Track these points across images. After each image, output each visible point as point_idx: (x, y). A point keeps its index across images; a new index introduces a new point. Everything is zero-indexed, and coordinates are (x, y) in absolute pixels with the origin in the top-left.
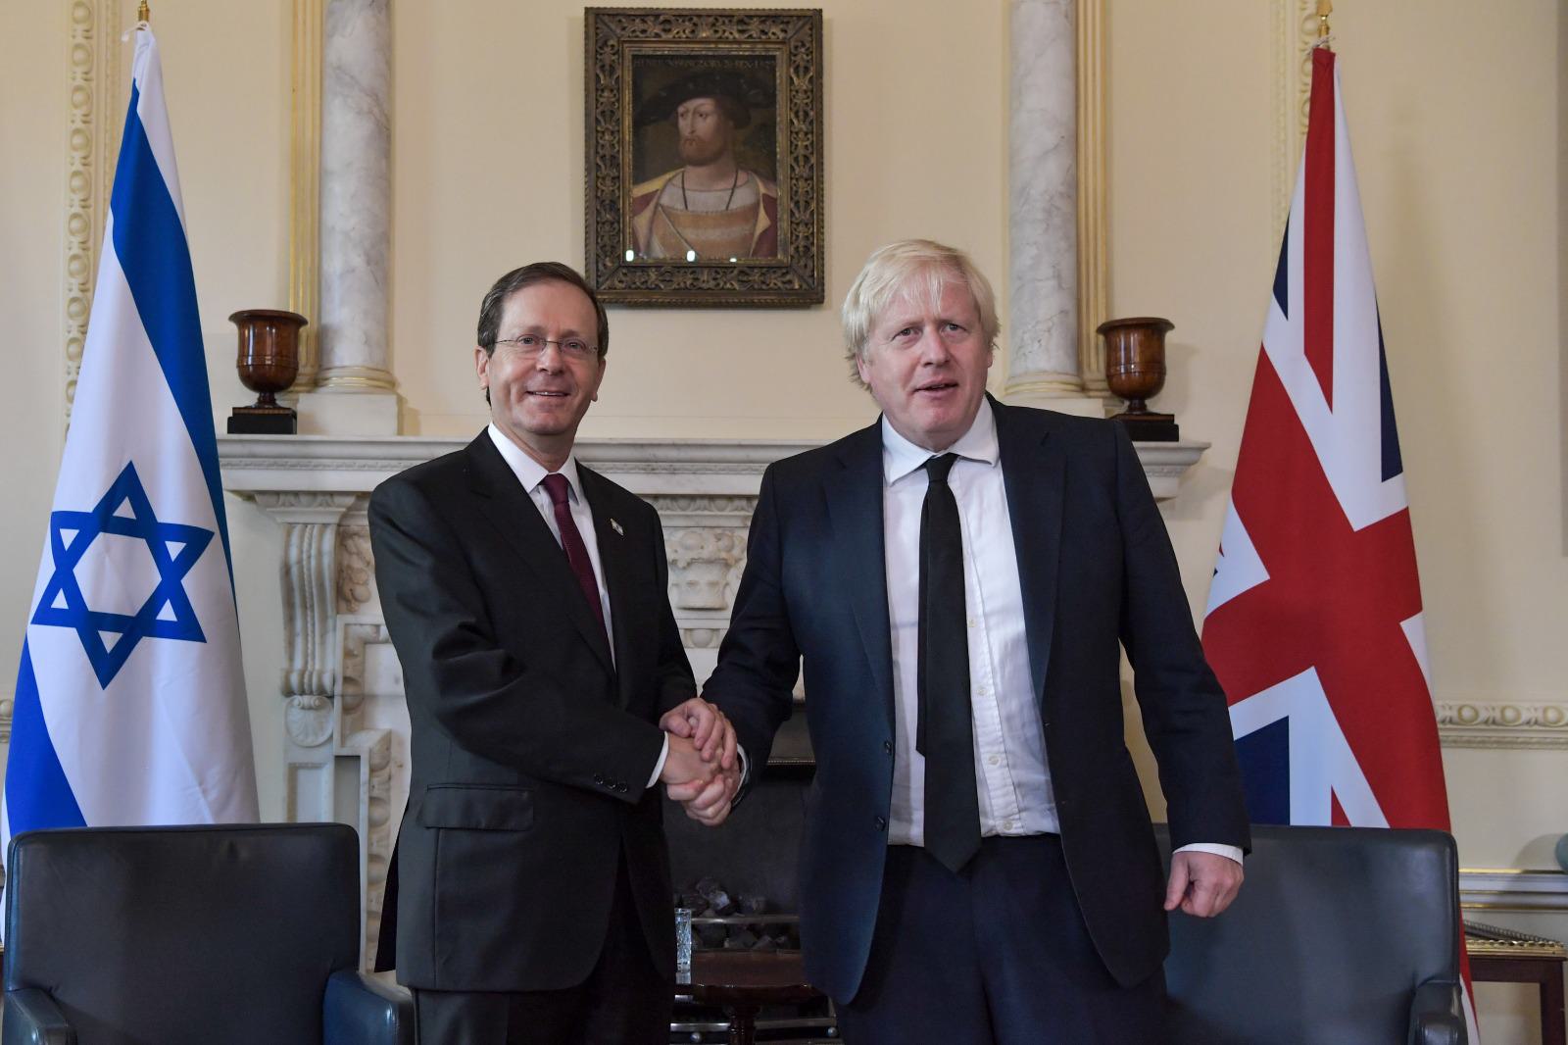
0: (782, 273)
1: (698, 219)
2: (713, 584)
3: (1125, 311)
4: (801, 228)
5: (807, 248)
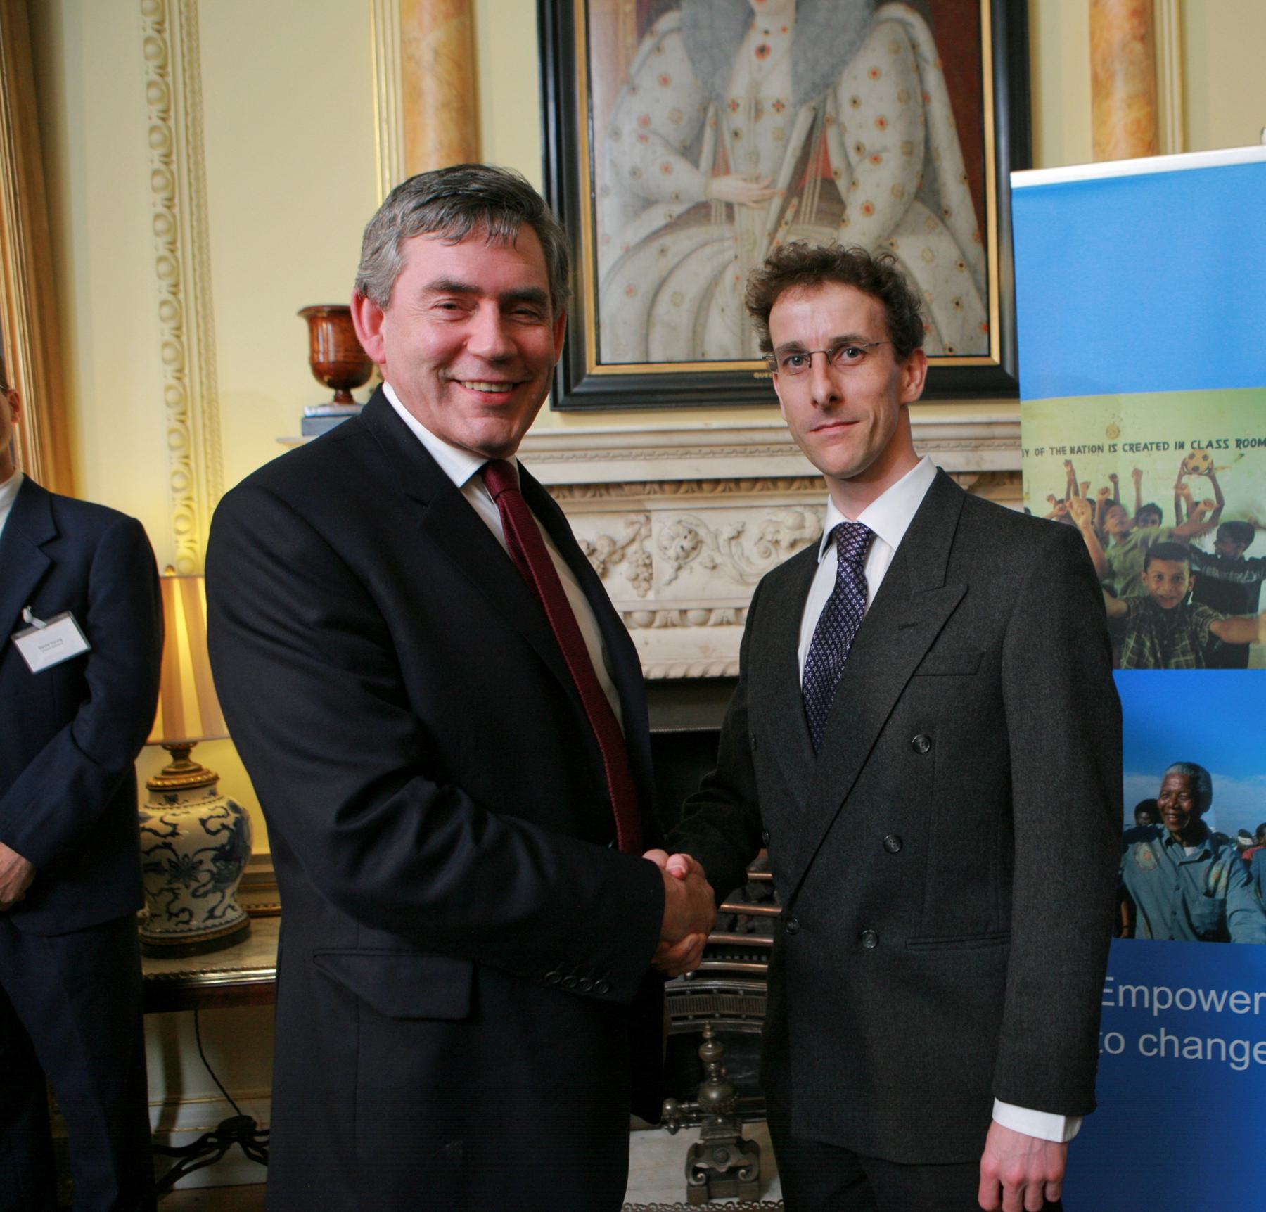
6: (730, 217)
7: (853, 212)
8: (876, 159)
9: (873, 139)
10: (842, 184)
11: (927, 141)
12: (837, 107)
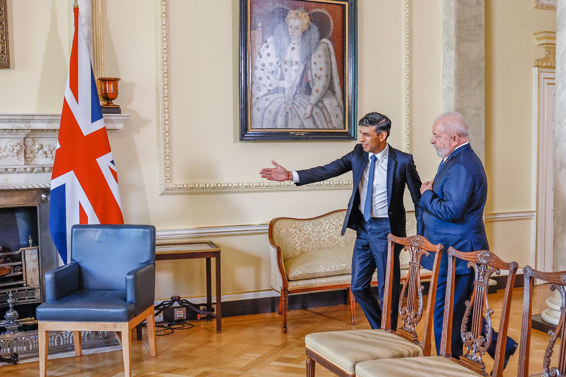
6: (284, 92)
7: (314, 92)
8: (319, 78)
9: (319, 73)
10: (311, 84)
11: (331, 74)
12: (311, 64)
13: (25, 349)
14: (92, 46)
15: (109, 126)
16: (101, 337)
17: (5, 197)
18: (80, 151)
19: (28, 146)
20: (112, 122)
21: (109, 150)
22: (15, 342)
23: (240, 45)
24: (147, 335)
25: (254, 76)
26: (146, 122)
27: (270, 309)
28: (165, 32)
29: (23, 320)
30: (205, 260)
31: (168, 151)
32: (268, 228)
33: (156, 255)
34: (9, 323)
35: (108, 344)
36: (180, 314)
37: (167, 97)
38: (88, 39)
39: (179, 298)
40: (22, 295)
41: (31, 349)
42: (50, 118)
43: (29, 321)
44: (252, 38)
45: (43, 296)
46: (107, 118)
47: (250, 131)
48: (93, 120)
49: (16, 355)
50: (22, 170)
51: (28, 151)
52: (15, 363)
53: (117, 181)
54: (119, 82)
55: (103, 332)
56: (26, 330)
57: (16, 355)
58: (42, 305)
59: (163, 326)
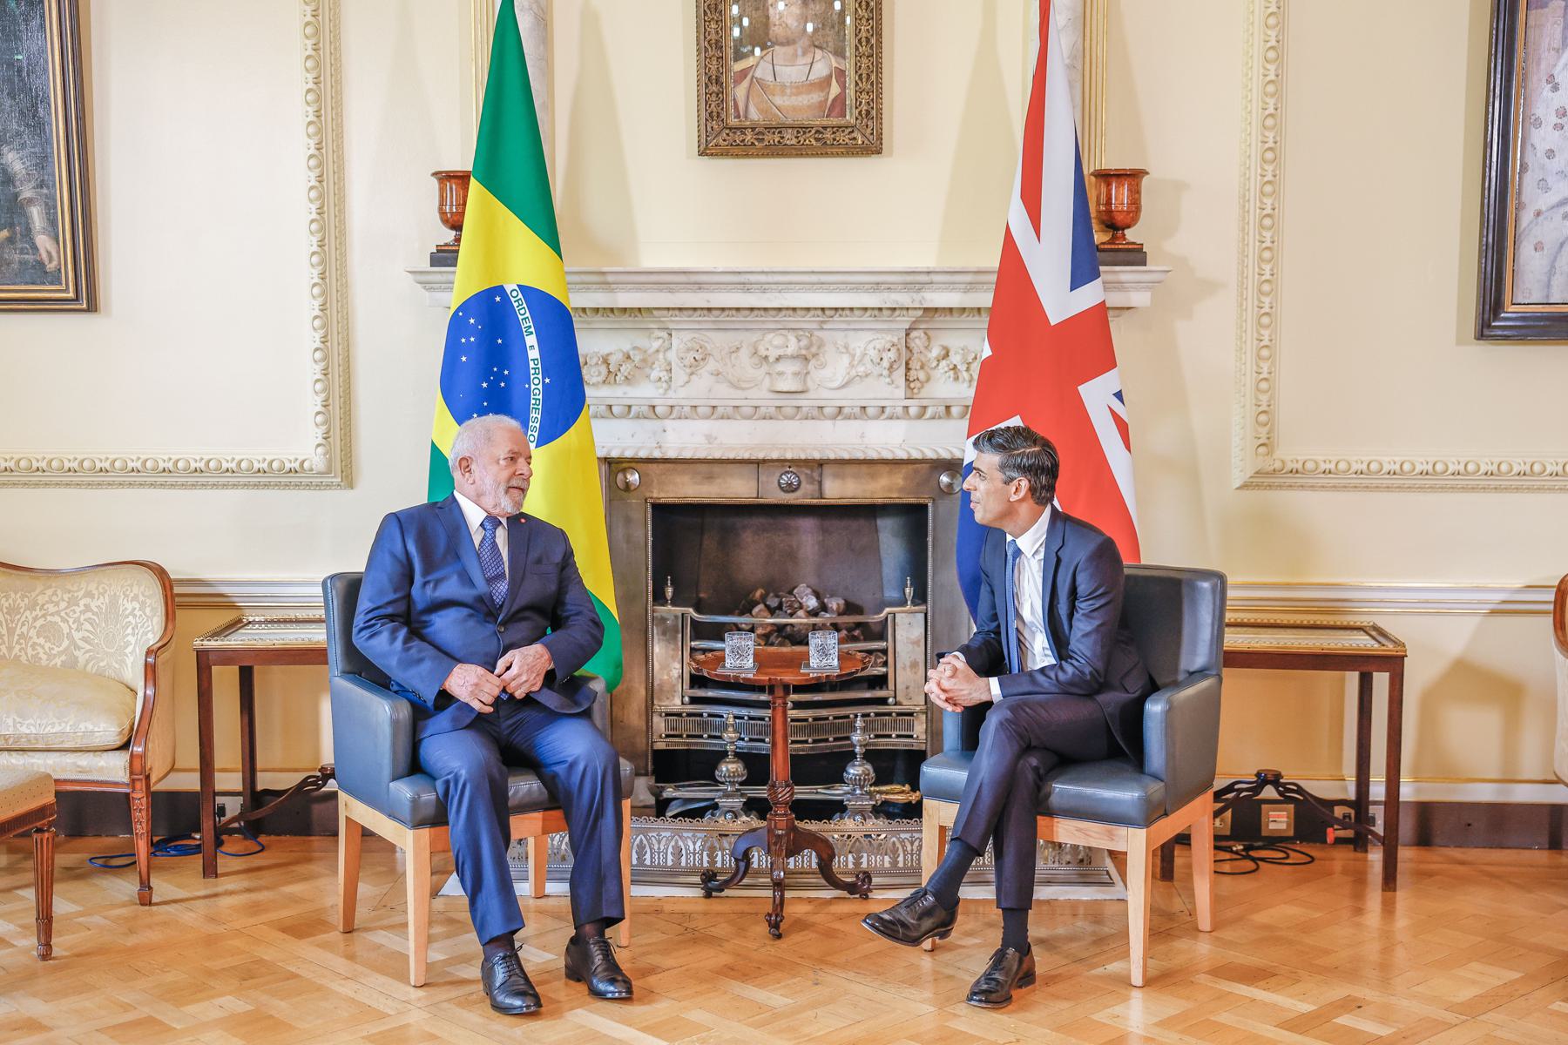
0: (850, 127)
1: (783, 87)
2: (796, 374)
3: (1111, 163)
4: (864, 95)
5: (868, 113)
13: (887, 865)
14: (1078, 86)
15: (1114, 300)
16: (1068, 858)
17: (856, 476)
18: (1039, 370)
19: (915, 351)
20: (1119, 290)
21: (1109, 363)
22: (865, 841)
23: (1492, 56)
24: (1189, 866)
25: (1529, 147)
26: (1209, 287)
27: (1544, 839)
28: (1272, 33)
29: (884, 788)
30: (1352, 679)
31: (1265, 367)
32: (1552, 597)
33: (1226, 653)
34: (852, 792)
35: (1086, 880)
36: (1278, 821)
37: (1270, 218)
38: (1071, 67)
39: (1278, 776)
40: (884, 726)
41: (901, 865)
42: (968, 278)
43: (898, 794)
44: (1531, 33)
45: (935, 733)
46: (1110, 277)
47: (1510, 310)
48: (1074, 286)
49: (867, 876)
50: (899, 410)
51: (914, 364)
52: (865, 896)
53: (1128, 447)
54: (1145, 181)
55: (1075, 848)
56: (890, 816)
57: (867, 876)
58: (930, 760)
59: (1229, 850)
